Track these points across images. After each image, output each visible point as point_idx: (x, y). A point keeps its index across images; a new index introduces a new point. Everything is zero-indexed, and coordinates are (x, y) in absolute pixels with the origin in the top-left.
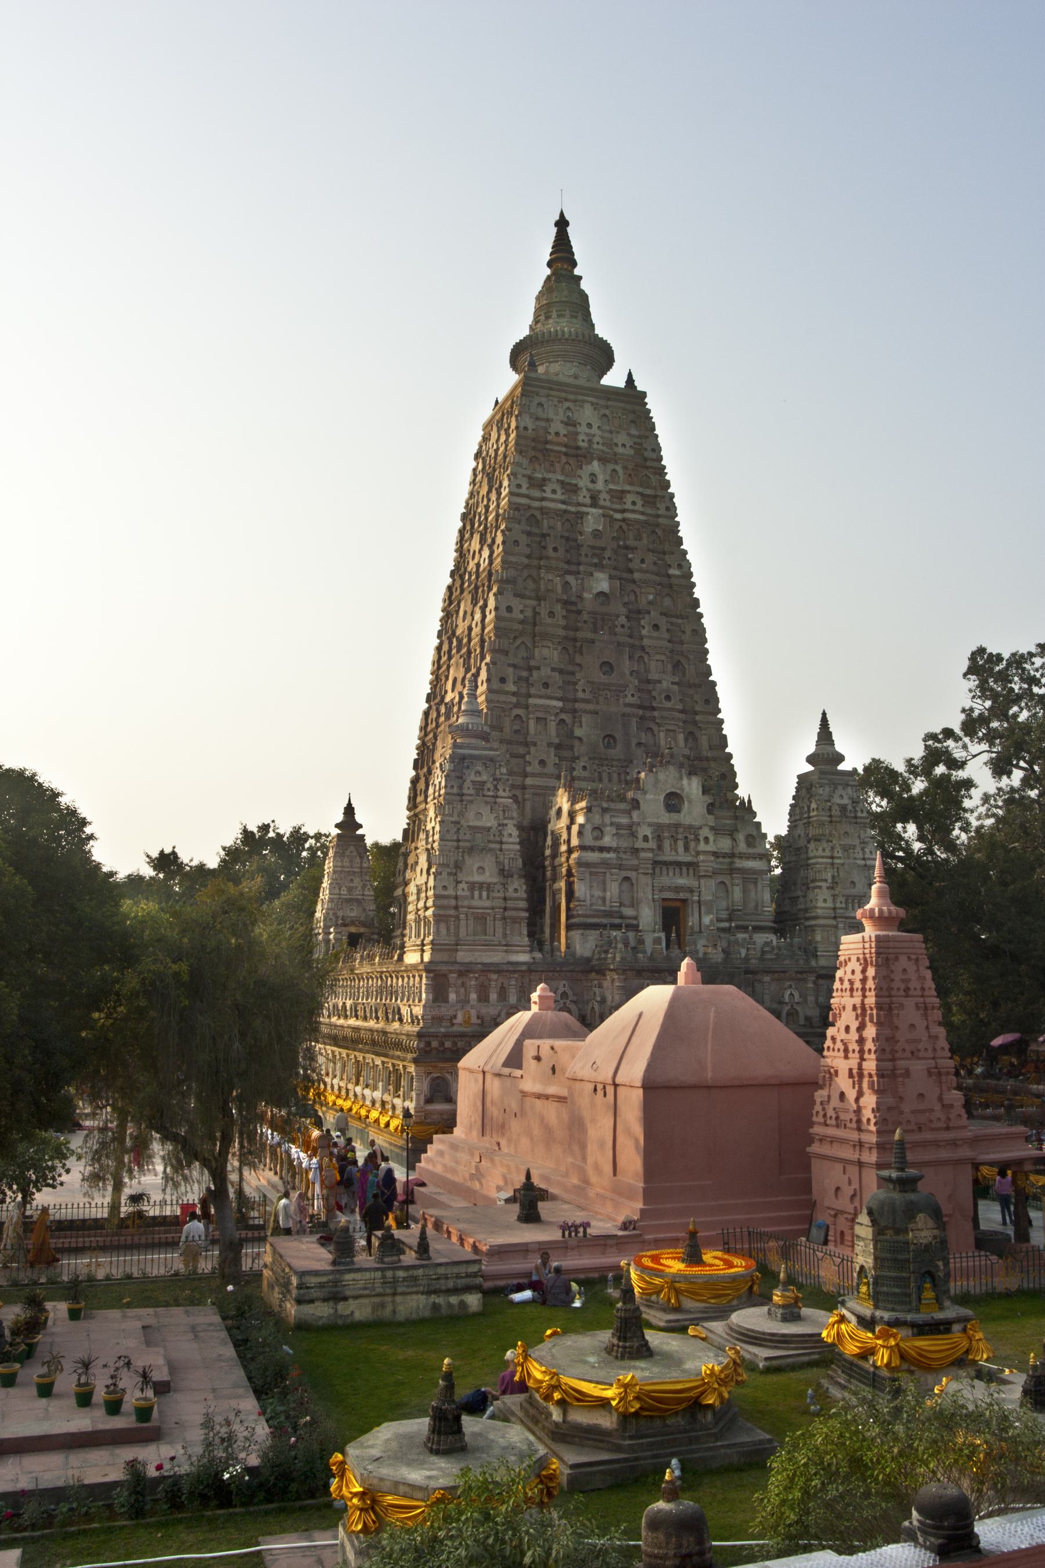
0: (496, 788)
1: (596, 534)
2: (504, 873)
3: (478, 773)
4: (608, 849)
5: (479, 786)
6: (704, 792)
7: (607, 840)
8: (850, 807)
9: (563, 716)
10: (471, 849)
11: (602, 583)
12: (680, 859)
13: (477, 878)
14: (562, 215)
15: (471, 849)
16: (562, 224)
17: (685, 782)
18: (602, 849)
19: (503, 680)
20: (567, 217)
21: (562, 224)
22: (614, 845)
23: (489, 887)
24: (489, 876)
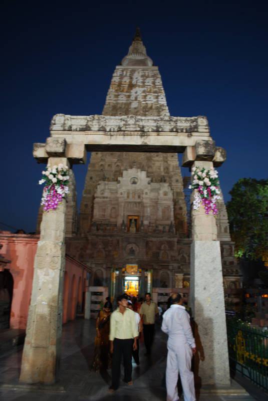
1: (135, 108)
4: (107, 198)
6: (148, 177)
9: (118, 164)
12: (136, 200)
18: (104, 198)
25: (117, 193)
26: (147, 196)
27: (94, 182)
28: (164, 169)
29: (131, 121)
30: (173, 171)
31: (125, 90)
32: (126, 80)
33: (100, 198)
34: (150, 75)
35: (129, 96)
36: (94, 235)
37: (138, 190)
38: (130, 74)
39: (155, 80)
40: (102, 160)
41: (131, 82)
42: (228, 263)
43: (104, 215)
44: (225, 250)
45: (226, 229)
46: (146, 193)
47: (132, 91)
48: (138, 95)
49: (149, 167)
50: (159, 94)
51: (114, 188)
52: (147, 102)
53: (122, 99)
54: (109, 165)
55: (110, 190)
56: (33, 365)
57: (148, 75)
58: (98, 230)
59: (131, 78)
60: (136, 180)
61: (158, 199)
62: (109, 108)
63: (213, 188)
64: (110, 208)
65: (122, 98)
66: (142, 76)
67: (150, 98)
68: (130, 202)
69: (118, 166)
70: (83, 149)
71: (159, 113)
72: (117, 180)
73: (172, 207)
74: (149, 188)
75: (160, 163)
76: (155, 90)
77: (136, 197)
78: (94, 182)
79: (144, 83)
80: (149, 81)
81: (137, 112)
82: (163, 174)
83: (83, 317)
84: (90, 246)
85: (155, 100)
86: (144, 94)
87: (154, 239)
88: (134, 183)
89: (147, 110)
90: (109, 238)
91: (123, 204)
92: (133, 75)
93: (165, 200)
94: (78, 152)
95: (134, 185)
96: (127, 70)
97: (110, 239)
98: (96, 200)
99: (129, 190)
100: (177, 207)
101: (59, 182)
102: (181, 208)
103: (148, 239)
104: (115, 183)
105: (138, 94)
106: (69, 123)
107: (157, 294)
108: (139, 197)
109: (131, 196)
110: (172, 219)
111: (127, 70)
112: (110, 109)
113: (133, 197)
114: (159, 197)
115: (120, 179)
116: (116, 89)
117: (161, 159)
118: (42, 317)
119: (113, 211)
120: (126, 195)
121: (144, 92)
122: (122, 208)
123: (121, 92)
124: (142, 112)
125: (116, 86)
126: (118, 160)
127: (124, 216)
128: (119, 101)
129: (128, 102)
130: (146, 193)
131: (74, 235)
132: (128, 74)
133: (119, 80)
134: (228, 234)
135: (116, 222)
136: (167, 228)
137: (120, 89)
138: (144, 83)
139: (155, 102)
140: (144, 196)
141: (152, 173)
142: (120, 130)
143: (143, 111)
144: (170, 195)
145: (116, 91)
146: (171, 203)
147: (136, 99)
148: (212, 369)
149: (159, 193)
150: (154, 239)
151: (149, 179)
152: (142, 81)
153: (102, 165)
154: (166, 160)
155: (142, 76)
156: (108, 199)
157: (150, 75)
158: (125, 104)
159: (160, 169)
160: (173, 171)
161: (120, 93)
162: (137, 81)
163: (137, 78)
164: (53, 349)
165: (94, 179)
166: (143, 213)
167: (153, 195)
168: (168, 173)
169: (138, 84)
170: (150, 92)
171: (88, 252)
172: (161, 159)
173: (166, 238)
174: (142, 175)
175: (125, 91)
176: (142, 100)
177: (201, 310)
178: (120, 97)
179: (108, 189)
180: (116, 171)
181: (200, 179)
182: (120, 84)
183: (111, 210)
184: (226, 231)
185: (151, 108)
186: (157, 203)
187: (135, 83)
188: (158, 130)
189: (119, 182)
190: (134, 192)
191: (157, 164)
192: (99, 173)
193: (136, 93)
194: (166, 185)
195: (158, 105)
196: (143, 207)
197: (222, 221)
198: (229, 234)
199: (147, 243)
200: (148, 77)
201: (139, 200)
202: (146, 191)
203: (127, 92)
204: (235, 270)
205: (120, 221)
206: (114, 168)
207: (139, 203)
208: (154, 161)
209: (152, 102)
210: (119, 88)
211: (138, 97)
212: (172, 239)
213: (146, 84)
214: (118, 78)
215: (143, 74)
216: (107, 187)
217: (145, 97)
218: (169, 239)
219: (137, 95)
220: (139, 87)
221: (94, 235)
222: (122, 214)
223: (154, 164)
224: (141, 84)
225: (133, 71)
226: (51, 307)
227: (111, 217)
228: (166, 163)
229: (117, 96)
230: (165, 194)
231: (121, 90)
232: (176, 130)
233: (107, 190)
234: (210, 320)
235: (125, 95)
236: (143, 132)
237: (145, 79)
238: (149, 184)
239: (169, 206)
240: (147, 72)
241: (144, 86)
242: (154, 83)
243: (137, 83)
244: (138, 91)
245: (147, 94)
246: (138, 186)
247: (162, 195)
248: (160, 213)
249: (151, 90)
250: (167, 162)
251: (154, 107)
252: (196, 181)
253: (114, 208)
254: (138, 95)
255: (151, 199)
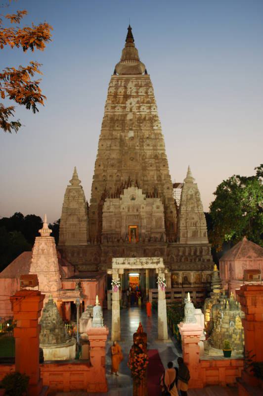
0: (79, 197)
1: (131, 120)
2: (79, 220)
3: (74, 193)
4: (112, 212)
5: (74, 197)
7: (111, 210)
8: (194, 195)
9: (118, 174)
10: (70, 215)
11: (131, 134)
12: (135, 214)
13: (71, 222)
14: (130, 26)
15: (70, 215)
16: (130, 29)
17: (137, 191)
18: (110, 212)
19: (99, 166)
20: (131, 27)
21: (130, 29)
22: (113, 211)
23: (75, 225)
24: (76, 222)
25: (120, 207)
26: (143, 210)
27: (98, 192)
28: (157, 177)
29: (138, 260)
30: (165, 180)
31: (121, 102)
32: (121, 90)
33: (107, 212)
34: (143, 84)
35: (125, 107)
36: (106, 246)
37: (136, 205)
38: (125, 84)
39: (148, 89)
40: (104, 171)
41: (125, 92)
42: (206, 261)
43: (111, 226)
44: (204, 250)
45: (205, 234)
46: (143, 208)
47: (127, 102)
48: (133, 107)
49: (144, 176)
50: (152, 105)
51: (117, 204)
52: (141, 113)
53: (119, 111)
54: (110, 176)
55: (115, 205)
56: (115, 336)
57: (141, 84)
58: (108, 242)
59: (125, 87)
60: (135, 197)
61: (152, 212)
62: (108, 120)
63: (164, 284)
64: (115, 220)
65: (118, 109)
66: (136, 85)
67: (143, 109)
68: (130, 215)
69: (118, 176)
70: (123, 270)
71: (152, 124)
72: (119, 197)
73: (163, 218)
74: (145, 203)
75: (153, 172)
76: (148, 99)
77: (135, 211)
78: (98, 192)
79: (137, 92)
80: (142, 91)
81: (133, 124)
82: (156, 182)
83: (107, 309)
84: (103, 255)
85: (148, 111)
86: (138, 105)
87: (149, 248)
88: (133, 199)
89: (141, 121)
90: (116, 248)
91: (125, 217)
92: (127, 85)
93: (157, 212)
94: (122, 272)
95: (133, 201)
96: (121, 79)
97: (118, 249)
98: (104, 214)
99: (129, 205)
100: (169, 211)
101: (118, 284)
102: (172, 212)
103: (145, 248)
104: (118, 199)
105: (132, 105)
106: (118, 262)
107: (151, 293)
108: (137, 210)
109: (131, 210)
110: (164, 227)
111: (121, 79)
112: (109, 122)
113: (133, 211)
114: (153, 210)
115: (121, 196)
116: (113, 100)
117: (155, 168)
118: (116, 323)
119: (118, 222)
120: (126, 210)
121: (138, 102)
122: (125, 221)
123: (117, 103)
124: (136, 123)
125: (112, 97)
126: (118, 171)
127: (126, 226)
128: (115, 113)
129: (124, 113)
130: (143, 208)
131: (89, 243)
132: (123, 84)
133: (114, 90)
134: (207, 238)
135: (121, 232)
136: (158, 236)
137: (116, 100)
138: (137, 92)
139: (148, 113)
140: (141, 210)
141: (147, 181)
142: (134, 263)
143: (138, 123)
144: (162, 209)
145: (113, 101)
146: (162, 215)
147: (131, 111)
148: (163, 335)
149: (152, 207)
150: (149, 248)
151: (144, 196)
152: (135, 90)
153: (104, 176)
154: (159, 169)
155: (136, 85)
156: (113, 214)
157: (143, 84)
158: (121, 115)
159: (153, 177)
160: (165, 180)
161: (116, 105)
162: (131, 91)
163: (131, 88)
164: (119, 332)
165: (98, 190)
166: (141, 224)
167: (148, 209)
168: (160, 180)
169: (132, 94)
170: (144, 103)
171: (102, 259)
172: (155, 168)
173: (158, 246)
174: (139, 192)
175: (121, 102)
176: (137, 111)
177: (160, 319)
178: (116, 109)
179: (113, 205)
180: (117, 181)
181: (160, 281)
182: (116, 95)
183: (116, 222)
184: (205, 236)
185: (145, 119)
186: (151, 214)
187: (129, 93)
188: (147, 263)
189: (121, 199)
190: (133, 207)
191: (152, 173)
192: (103, 183)
193: (131, 104)
194: (158, 200)
195: (151, 116)
196: (141, 219)
197: (201, 228)
198: (207, 238)
199: (145, 251)
200: (141, 87)
201: (137, 214)
202: (143, 205)
203: (122, 103)
204: (210, 266)
205: (124, 231)
206: (115, 178)
207: (137, 215)
208: (148, 170)
209: (146, 113)
210: (115, 99)
211: (133, 108)
212: (162, 247)
213: (140, 94)
214: (114, 88)
215: (137, 83)
216: (111, 204)
217: (139, 107)
218: (161, 247)
219: (132, 105)
220: (133, 98)
221: (106, 246)
222: (125, 225)
223: (149, 173)
224: (135, 94)
225: (127, 81)
226: (118, 321)
227: (116, 228)
228: (158, 172)
229: (114, 108)
230: (158, 208)
231: (117, 101)
232: (153, 263)
233: (112, 206)
234: (163, 322)
235: (121, 107)
236: (142, 263)
237: (138, 89)
238: (145, 199)
239: (161, 218)
240: (140, 80)
241: (137, 96)
242: (146, 93)
243: (131, 93)
244: (133, 101)
245: (141, 105)
246: (136, 202)
247: (155, 209)
248: (154, 223)
249: (144, 100)
250: (159, 171)
251: (147, 119)
252: (159, 281)
253: (118, 220)
254: (133, 107)
255: (146, 212)
